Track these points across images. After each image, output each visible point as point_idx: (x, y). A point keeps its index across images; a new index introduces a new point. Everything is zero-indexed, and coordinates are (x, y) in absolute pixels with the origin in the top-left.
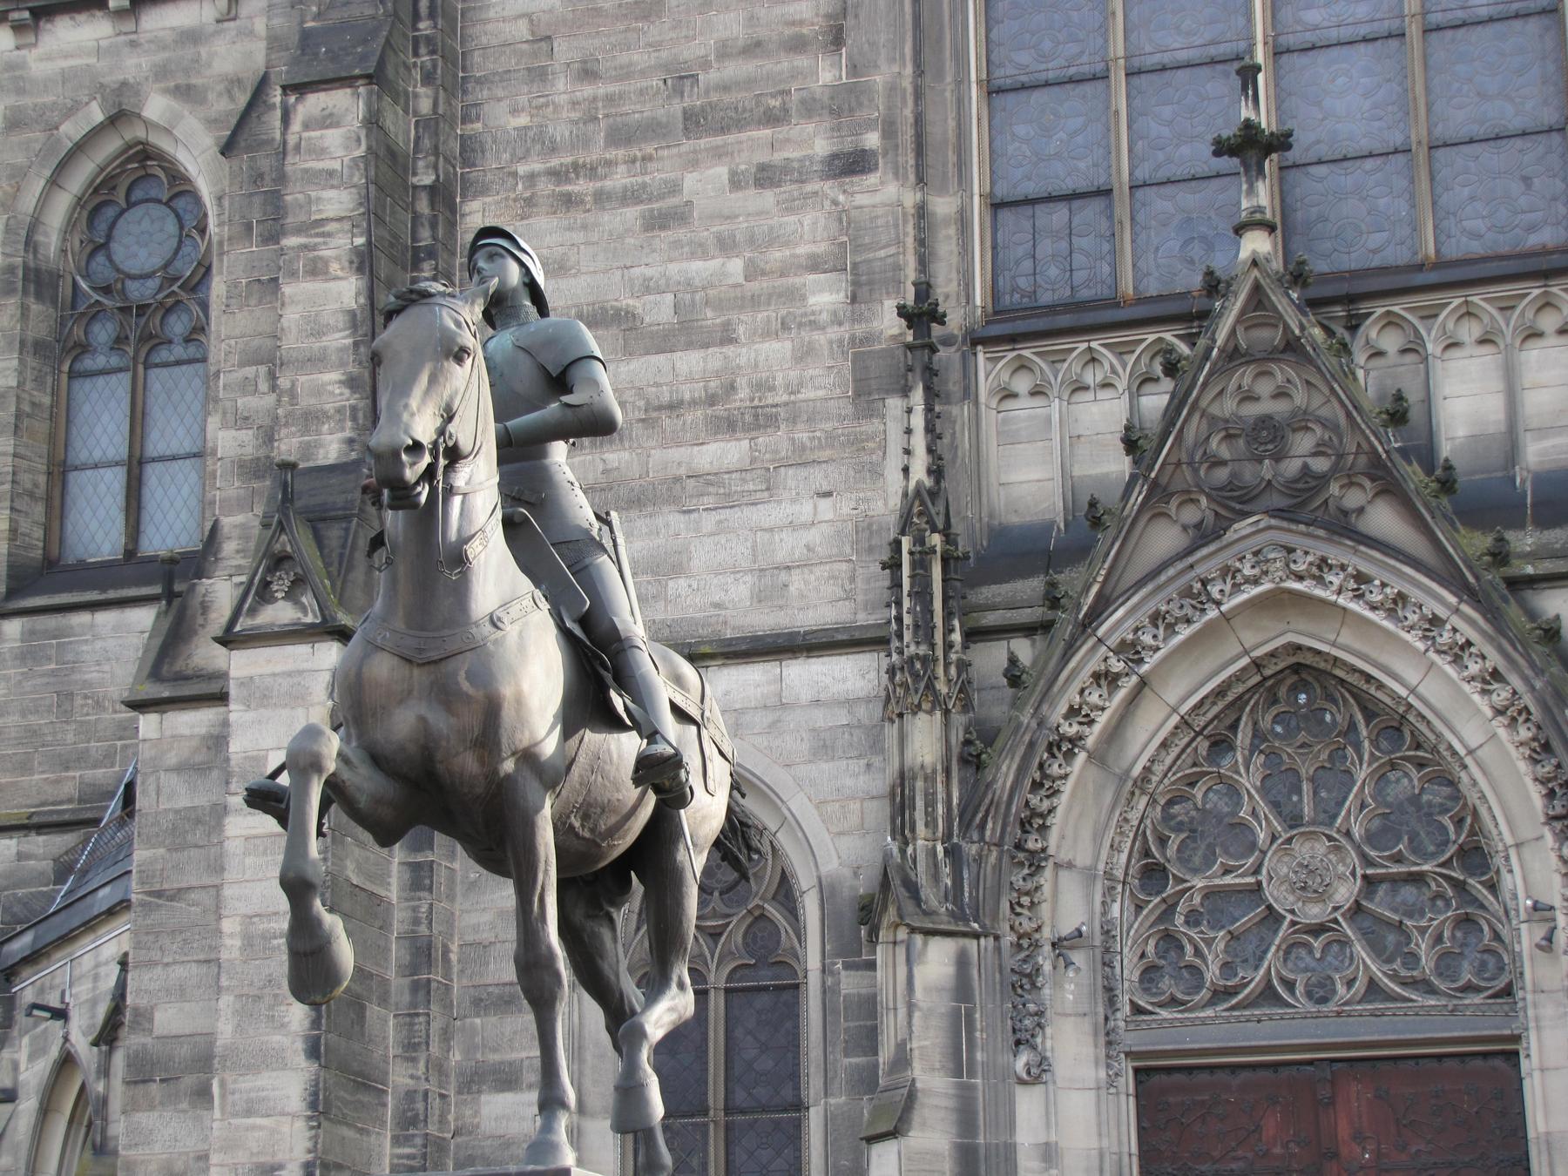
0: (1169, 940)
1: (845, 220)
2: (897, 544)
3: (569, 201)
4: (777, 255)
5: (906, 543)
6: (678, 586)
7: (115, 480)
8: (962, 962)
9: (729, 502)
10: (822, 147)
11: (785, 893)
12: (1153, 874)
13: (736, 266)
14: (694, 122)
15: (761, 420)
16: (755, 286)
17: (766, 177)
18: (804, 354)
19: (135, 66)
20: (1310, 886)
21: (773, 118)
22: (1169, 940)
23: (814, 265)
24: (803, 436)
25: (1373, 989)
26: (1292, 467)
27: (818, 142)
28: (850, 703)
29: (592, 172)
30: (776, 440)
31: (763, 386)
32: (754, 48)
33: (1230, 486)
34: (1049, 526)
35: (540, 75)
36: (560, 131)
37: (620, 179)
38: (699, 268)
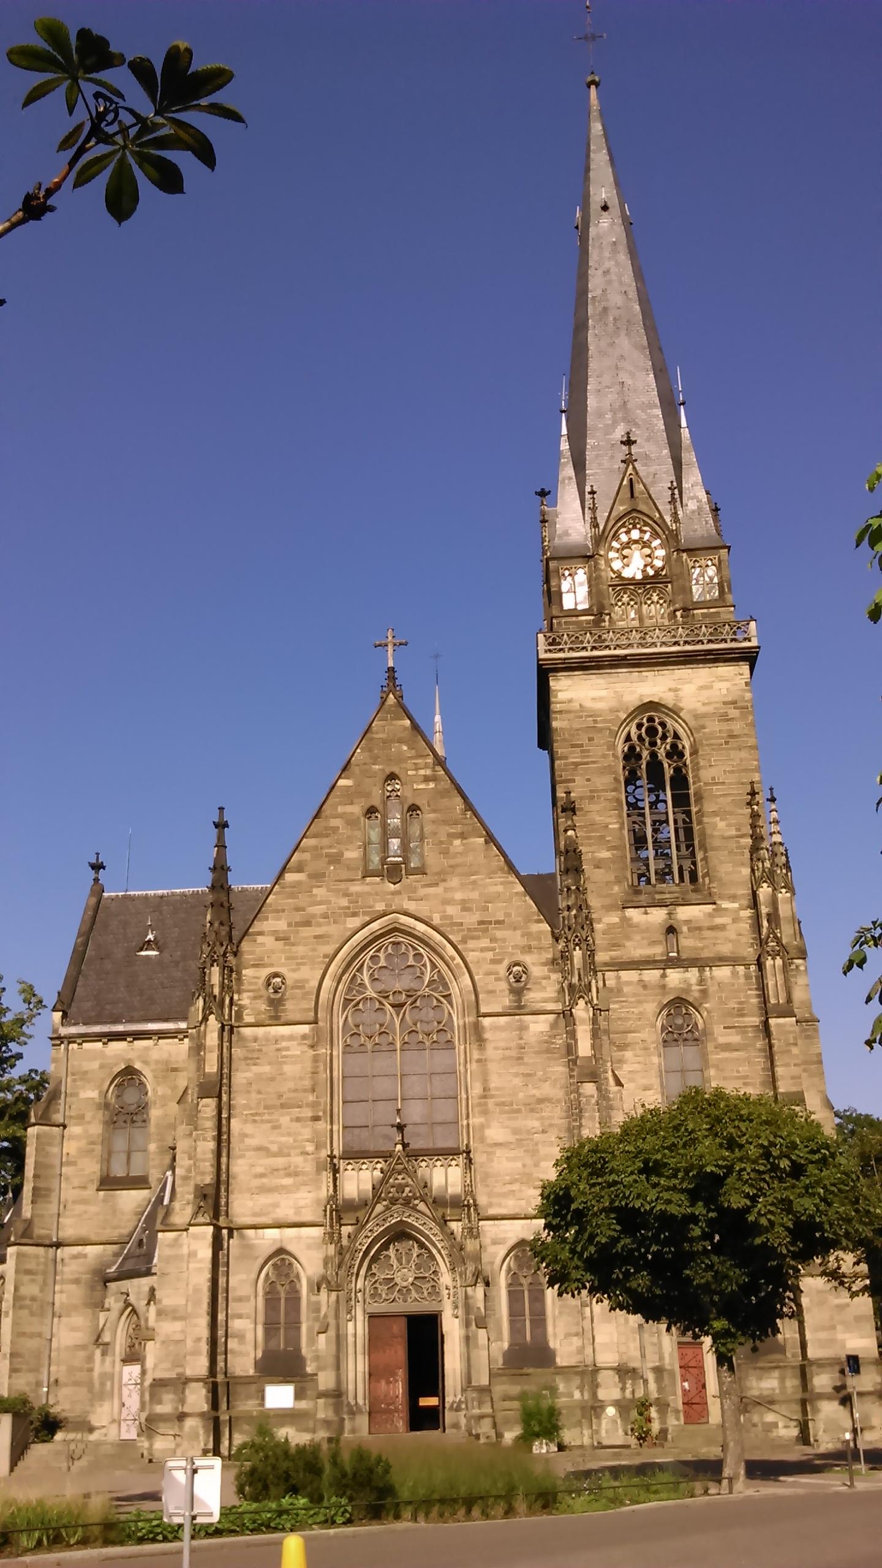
1: (315, 1132)
2: (326, 1207)
3: (255, 1121)
4: (300, 1138)
5: (328, 1206)
6: (278, 1210)
7: (124, 1157)
8: (338, 1297)
9: (289, 1192)
10: (310, 1114)
13: (291, 1140)
14: (283, 1106)
15: (296, 1174)
16: (296, 1144)
17: (298, 1120)
18: (306, 1161)
19: (132, 1055)
21: (300, 1107)
23: (308, 1140)
24: (305, 1178)
25: (416, 1299)
26: (404, 1195)
27: (308, 1113)
28: (313, 1238)
30: (300, 1179)
31: (297, 1167)
32: (296, 1090)
33: (392, 1198)
37: (266, 1117)
38: (283, 1139)
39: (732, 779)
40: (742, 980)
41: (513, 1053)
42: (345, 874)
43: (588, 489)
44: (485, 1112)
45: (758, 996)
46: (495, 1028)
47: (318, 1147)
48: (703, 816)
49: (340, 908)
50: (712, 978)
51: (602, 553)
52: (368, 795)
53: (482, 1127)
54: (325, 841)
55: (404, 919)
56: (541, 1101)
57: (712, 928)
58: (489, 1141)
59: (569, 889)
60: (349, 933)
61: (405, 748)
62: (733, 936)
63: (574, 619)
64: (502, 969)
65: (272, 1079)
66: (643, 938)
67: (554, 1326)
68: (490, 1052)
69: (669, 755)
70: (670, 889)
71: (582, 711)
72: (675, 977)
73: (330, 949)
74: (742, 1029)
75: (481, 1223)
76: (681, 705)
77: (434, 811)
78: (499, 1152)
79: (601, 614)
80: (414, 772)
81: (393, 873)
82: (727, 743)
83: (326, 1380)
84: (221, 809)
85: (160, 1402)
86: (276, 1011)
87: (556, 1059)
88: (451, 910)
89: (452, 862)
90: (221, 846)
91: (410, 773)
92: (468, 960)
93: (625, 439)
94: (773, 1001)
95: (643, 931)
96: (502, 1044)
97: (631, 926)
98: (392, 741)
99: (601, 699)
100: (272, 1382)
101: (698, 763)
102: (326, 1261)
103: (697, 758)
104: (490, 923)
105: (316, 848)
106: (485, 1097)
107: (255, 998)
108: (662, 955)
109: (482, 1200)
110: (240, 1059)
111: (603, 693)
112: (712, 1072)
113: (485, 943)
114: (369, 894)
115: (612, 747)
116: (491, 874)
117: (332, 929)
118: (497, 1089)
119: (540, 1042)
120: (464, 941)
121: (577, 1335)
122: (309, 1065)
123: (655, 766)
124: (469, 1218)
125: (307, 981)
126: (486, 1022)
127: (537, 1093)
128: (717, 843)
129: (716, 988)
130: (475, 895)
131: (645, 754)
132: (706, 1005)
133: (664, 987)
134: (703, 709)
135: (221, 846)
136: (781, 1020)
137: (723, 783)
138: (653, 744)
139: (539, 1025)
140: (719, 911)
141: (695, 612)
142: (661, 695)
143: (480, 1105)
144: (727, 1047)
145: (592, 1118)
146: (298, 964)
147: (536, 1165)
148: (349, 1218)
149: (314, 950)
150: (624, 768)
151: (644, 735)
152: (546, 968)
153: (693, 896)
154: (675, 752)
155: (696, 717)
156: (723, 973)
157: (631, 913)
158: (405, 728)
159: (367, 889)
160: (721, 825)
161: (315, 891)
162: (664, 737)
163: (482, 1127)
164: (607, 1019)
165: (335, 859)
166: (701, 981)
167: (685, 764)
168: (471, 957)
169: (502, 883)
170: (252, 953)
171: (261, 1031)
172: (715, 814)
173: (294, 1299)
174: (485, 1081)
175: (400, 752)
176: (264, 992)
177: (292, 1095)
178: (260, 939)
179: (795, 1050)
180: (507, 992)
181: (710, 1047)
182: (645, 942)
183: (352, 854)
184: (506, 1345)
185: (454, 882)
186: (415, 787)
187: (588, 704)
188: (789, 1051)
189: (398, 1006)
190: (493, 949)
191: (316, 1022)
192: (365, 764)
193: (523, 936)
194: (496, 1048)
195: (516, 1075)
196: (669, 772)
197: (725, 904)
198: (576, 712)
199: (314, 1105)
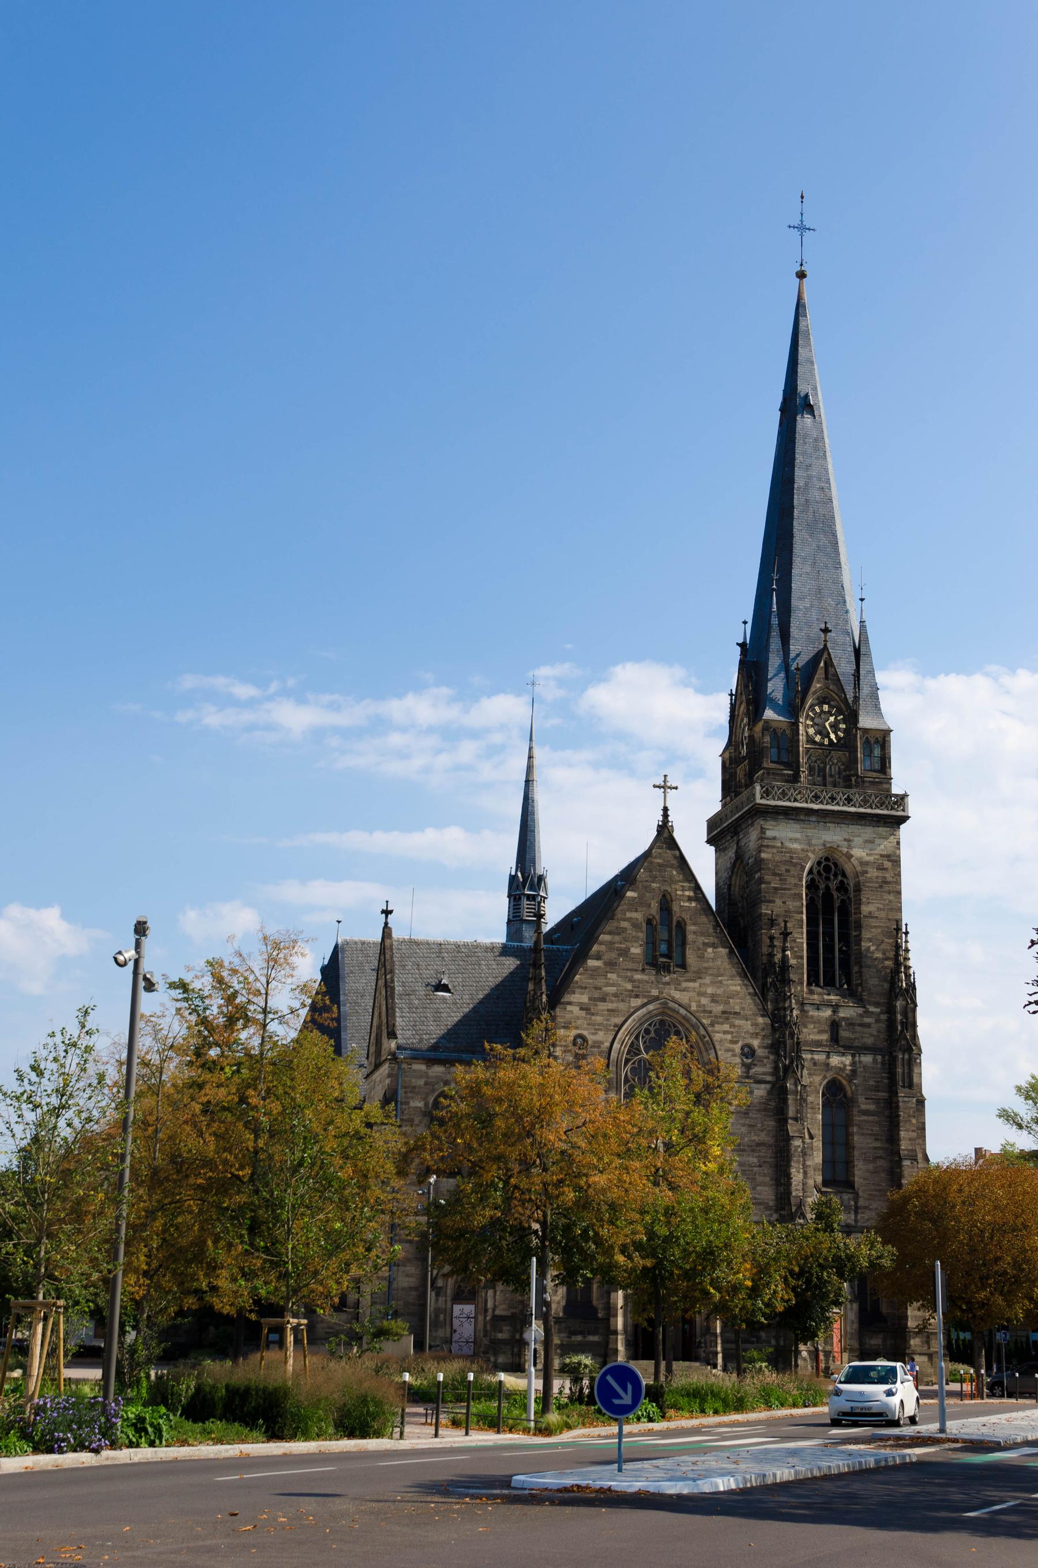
39: (883, 914)
40: (879, 1066)
42: (630, 966)
45: (889, 1078)
49: (626, 990)
50: (860, 1062)
52: (649, 906)
54: (617, 938)
56: (759, 1144)
57: (862, 1025)
60: (632, 1010)
61: (675, 873)
62: (875, 1033)
64: (737, 1048)
69: (838, 889)
71: (782, 848)
73: (618, 1020)
74: (877, 1101)
77: (695, 924)
82: (881, 887)
85: (501, 1331)
87: (770, 1116)
88: (704, 1001)
89: (705, 965)
93: (823, 626)
95: (814, 1023)
98: (667, 866)
99: (796, 840)
101: (860, 900)
103: (860, 895)
104: (730, 1013)
105: (612, 943)
107: (565, 1051)
111: (798, 835)
112: (855, 1129)
113: (726, 1027)
114: (647, 982)
116: (732, 977)
117: (622, 1006)
119: (760, 1103)
120: (712, 1025)
123: (828, 894)
125: (602, 1043)
127: (756, 1138)
129: (862, 1069)
130: (720, 991)
131: (822, 886)
132: (855, 1081)
133: (828, 1065)
134: (868, 858)
138: (828, 879)
140: (867, 1013)
142: (839, 843)
144: (866, 1113)
145: (798, 1162)
146: (595, 1029)
149: (608, 1020)
151: (822, 871)
154: (842, 888)
156: (867, 1059)
159: (645, 977)
161: (609, 975)
162: (836, 875)
165: (625, 953)
166: (853, 1064)
167: (849, 897)
172: (870, 940)
175: (671, 876)
176: (571, 1047)
178: (569, 1008)
179: (914, 1121)
181: (855, 1111)
182: (816, 1030)
185: (707, 980)
186: (682, 904)
188: (910, 1121)
190: (732, 1033)
192: (647, 881)
193: (752, 1025)
195: (744, 1125)
196: (837, 904)
197: (872, 1009)
198: (778, 847)
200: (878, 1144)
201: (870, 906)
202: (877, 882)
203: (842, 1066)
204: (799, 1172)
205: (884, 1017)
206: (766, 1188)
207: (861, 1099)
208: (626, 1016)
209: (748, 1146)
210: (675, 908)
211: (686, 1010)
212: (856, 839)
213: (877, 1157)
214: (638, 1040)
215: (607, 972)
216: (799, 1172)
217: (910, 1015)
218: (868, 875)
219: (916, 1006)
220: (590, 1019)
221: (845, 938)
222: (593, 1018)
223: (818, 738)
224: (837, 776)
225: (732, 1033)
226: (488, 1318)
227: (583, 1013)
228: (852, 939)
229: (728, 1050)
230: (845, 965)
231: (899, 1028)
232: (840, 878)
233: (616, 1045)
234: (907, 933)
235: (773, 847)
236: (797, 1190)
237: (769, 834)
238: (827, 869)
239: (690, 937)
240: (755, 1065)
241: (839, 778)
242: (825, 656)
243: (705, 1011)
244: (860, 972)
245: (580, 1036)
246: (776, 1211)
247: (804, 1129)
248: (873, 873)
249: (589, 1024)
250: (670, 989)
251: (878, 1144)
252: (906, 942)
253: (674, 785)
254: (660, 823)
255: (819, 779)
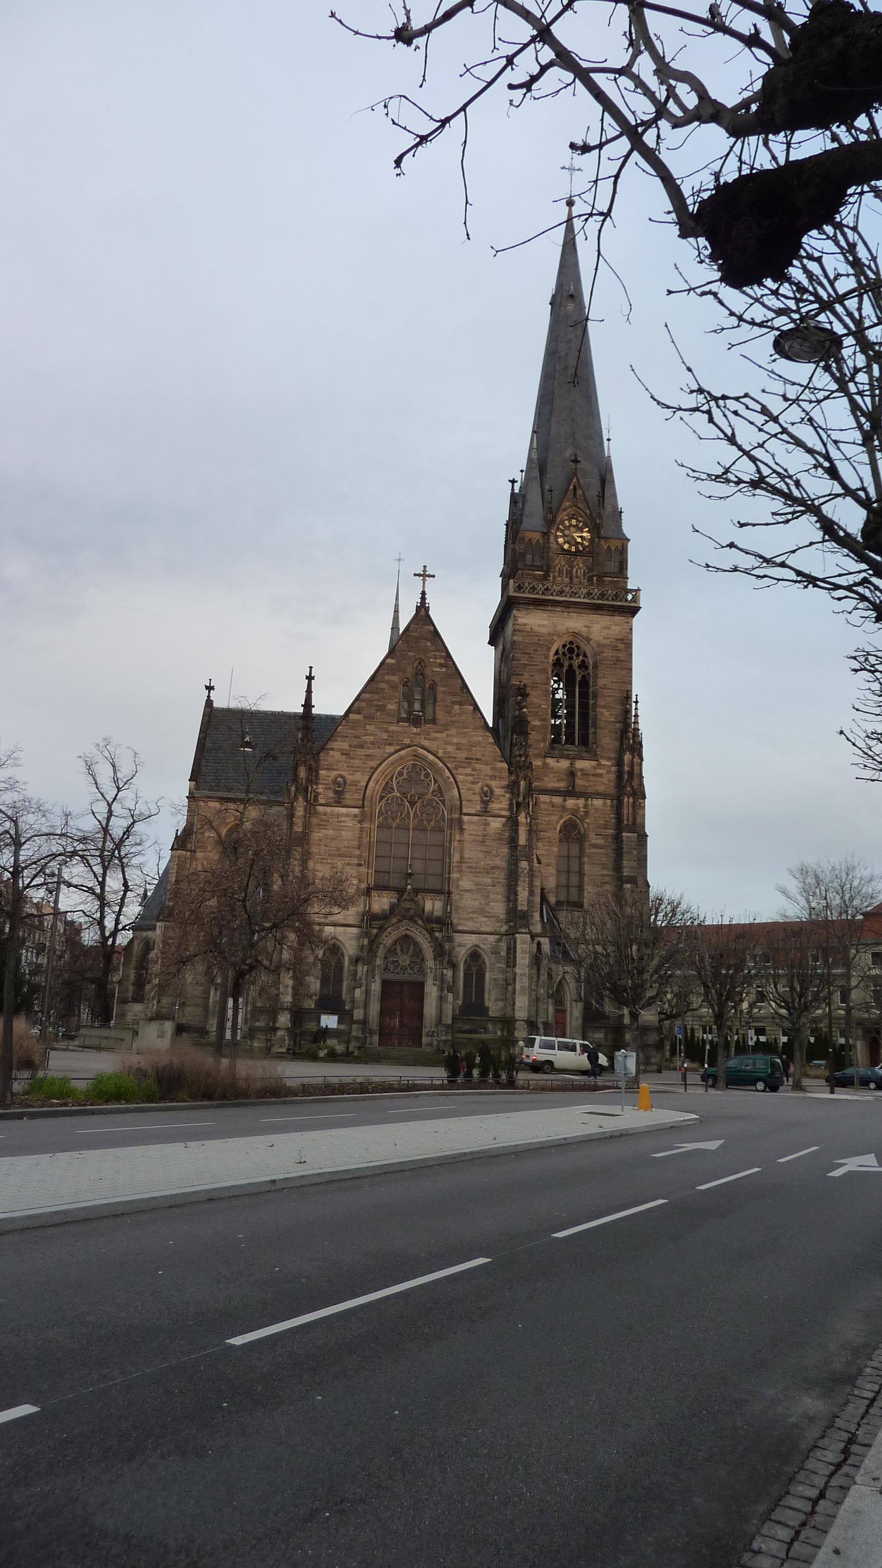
0: (387, 966)
1: (358, 872)
3: (323, 863)
10: (356, 862)
11: (343, 955)
12: (386, 958)
14: (339, 855)
20: (404, 961)
22: (387, 966)
29: (325, 859)
32: (348, 847)
34: (378, 914)
35: (320, 845)
36: (322, 853)
37: (329, 861)
41: (480, 838)
43: (547, 487)
44: (460, 871)
45: (616, 818)
46: (471, 823)
47: (360, 881)
48: (596, 707)
49: (382, 739)
51: (552, 531)
52: (405, 671)
53: (458, 879)
54: (376, 696)
55: (421, 751)
56: (493, 868)
57: (593, 775)
58: (461, 888)
59: (521, 744)
60: (386, 755)
61: (429, 644)
62: (606, 782)
63: (532, 572)
64: (477, 788)
65: (335, 839)
66: (554, 777)
67: (489, 994)
68: (466, 836)
69: (579, 667)
70: (572, 750)
72: (571, 802)
73: (373, 764)
74: (605, 837)
75: (454, 934)
76: (591, 637)
77: (444, 686)
78: (466, 894)
79: (549, 571)
80: (434, 660)
81: (416, 721)
82: (615, 664)
83: (358, 1014)
84: (311, 668)
86: (339, 798)
88: (450, 748)
89: (452, 719)
90: (309, 692)
91: (431, 660)
92: (458, 780)
93: (573, 458)
94: (625, 822)
96: (474, 833)
97: (548, 768)
99: (543, 626)
100: (325, 1013)
101: (597, 674)
102: (362, 948)
104: (472, 759)
105: (370, 700)
106: (461, 862)
107: (326, 789)
108: (564, 788)
109: (455, 921)
110: (315, 825)
111: (545, 622)
112: (586, 859)
113: (468, 771)
114: (401, 733)
115: (547, 657)
117: (376, 752)
118: (469, 859)
119: (496, 833)
120: (456, 768)
121: (501, 1000)
122: (357, 832)
123: (571, 671)
124: (448, 930)
126: (465, 818)
128: (602, 724)
130: (464, 741)
131: (566, 664)
133: (564, 807)
135: (309, 692)
136: (629, 834)
137: (610, 689)
138: (571, 658)
139: (496, 824)
140: (600, 765)
141: (606, 579)
143: (457, 867)
144: (596, 846)
145: (524, 881)
146: (354, 771)
147: (487, 904)
148: (377, 923)
150: (552, 671)
151: (566, 652)
152: (503, 790)
153: (585, 754)
154: (583, 665)
155: (599, 645)
156: (598, 803)
157: (549, 761)
158: (430, 632)
160: (607, 714)
161: (367, 727)
162: (578, 655)
163: (458, 879)
164: (536, 824)
165: (382, 709)
166: (586, 806)
167: (588, 673)
168: (460, 778)
169: (481, 736)
170: (327, 761)
171: (329, 809)
172: (604, 707)
173: (340, 967)
174: (462, 853)
176: (332, 786)
177: (345, 849)
178: (331, 753)
180: (479, 802)
183: (392, 707)
184: (461, 1002)
185: (453, 731)
187: (536, 628)
189: (412, 804)
190: (473, 775)
191: (363, 807)
193: (491, 769)
194: (469, 835)
195: (481, 851)
196: (578, 679)
197: (604, 762)
198: (528, 632)
199: (359, 857)
200: (606, 872)
201: (605, 680)
202: (613, 661)
203: (576, 808)
204: (525, 890)
205: (614, 769)
206: (498, 904)
207: (592, 835)
208: (382, 759)
209: (483, 869)
210: (428, 672)
211: (434, 755)
212: (595, 625)
213: (604, 883)
214: (391, 780)
215: (366, 724)
216: (525, 890)
217: (636, 768)
218: (604, 655)
219: (642, 760)
220: (350, 762)
221: (584, 706)
222: (352, 761)
223: (566, 546)
224: (582, 578)
225: (473, 775)
226: (249, 1009)
227: (344, 758)
228: (590, 707)
229: (469, 790)
230: (584, 726)
231: (626, 777)
232: (581, 658)
233: (371, 784)
234: (636, 702)
235: (523, 631)
236: (522, 905)
237: (520, 621)
238: (571, 651)
239: (439, 697)
240: (492, 802)
241: (584, 579)
242: (575, 480)
243: (450, 757)
244: (595, 733)
245: (341, 776)
246: (506, 923)
247: (533, 855)
248: (608, 653)
249: (347, 767)
250: (420, 738)
251: (606, 872)
252: (636, 709)
253: (431, 574)
254: (419, 605)
255: (567, 579)
